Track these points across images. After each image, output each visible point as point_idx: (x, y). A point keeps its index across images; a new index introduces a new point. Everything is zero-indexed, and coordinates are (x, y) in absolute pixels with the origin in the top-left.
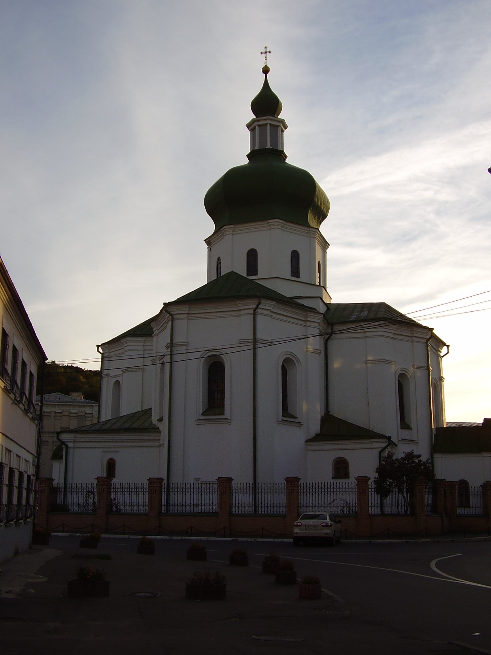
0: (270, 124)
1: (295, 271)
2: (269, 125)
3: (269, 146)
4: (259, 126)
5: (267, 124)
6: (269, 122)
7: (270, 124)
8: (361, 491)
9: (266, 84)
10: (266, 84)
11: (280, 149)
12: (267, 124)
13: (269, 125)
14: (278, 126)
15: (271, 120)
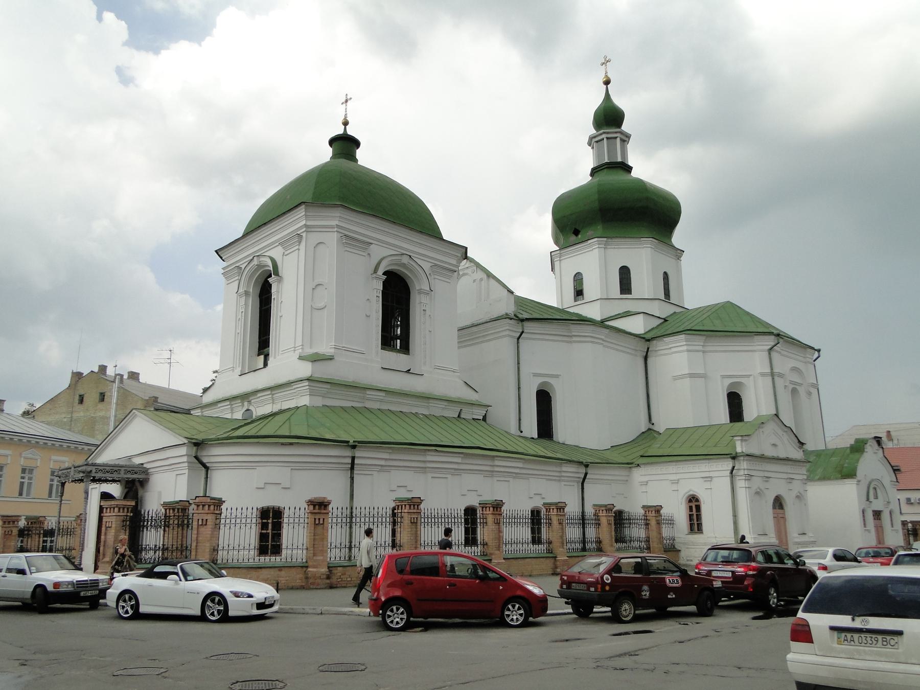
0: (607, 138)
1: (625, 285)
2: (605, 139)
3: (606, 161)
4: (597, 142)
5: (603, 139)
6: (604, 136)
7: (607, 138)
8: (317, 522)
9: (607, 95)
10: (607, 95)
11: (619, 160)
12: (603, 139)
13: (605, 139)
14: (616, 138)
15: (608, 133)
